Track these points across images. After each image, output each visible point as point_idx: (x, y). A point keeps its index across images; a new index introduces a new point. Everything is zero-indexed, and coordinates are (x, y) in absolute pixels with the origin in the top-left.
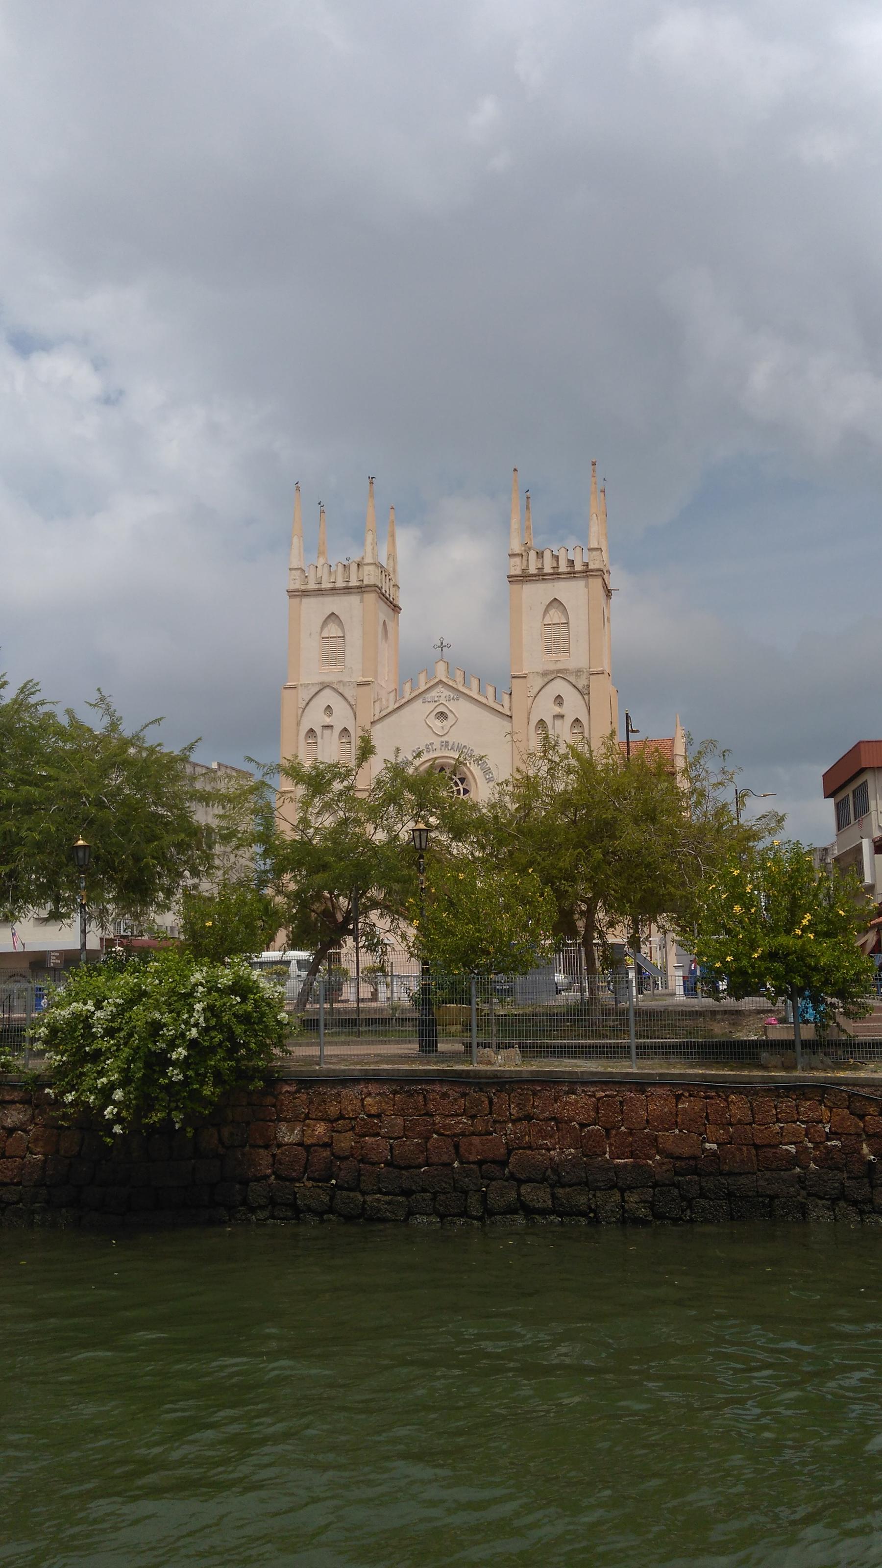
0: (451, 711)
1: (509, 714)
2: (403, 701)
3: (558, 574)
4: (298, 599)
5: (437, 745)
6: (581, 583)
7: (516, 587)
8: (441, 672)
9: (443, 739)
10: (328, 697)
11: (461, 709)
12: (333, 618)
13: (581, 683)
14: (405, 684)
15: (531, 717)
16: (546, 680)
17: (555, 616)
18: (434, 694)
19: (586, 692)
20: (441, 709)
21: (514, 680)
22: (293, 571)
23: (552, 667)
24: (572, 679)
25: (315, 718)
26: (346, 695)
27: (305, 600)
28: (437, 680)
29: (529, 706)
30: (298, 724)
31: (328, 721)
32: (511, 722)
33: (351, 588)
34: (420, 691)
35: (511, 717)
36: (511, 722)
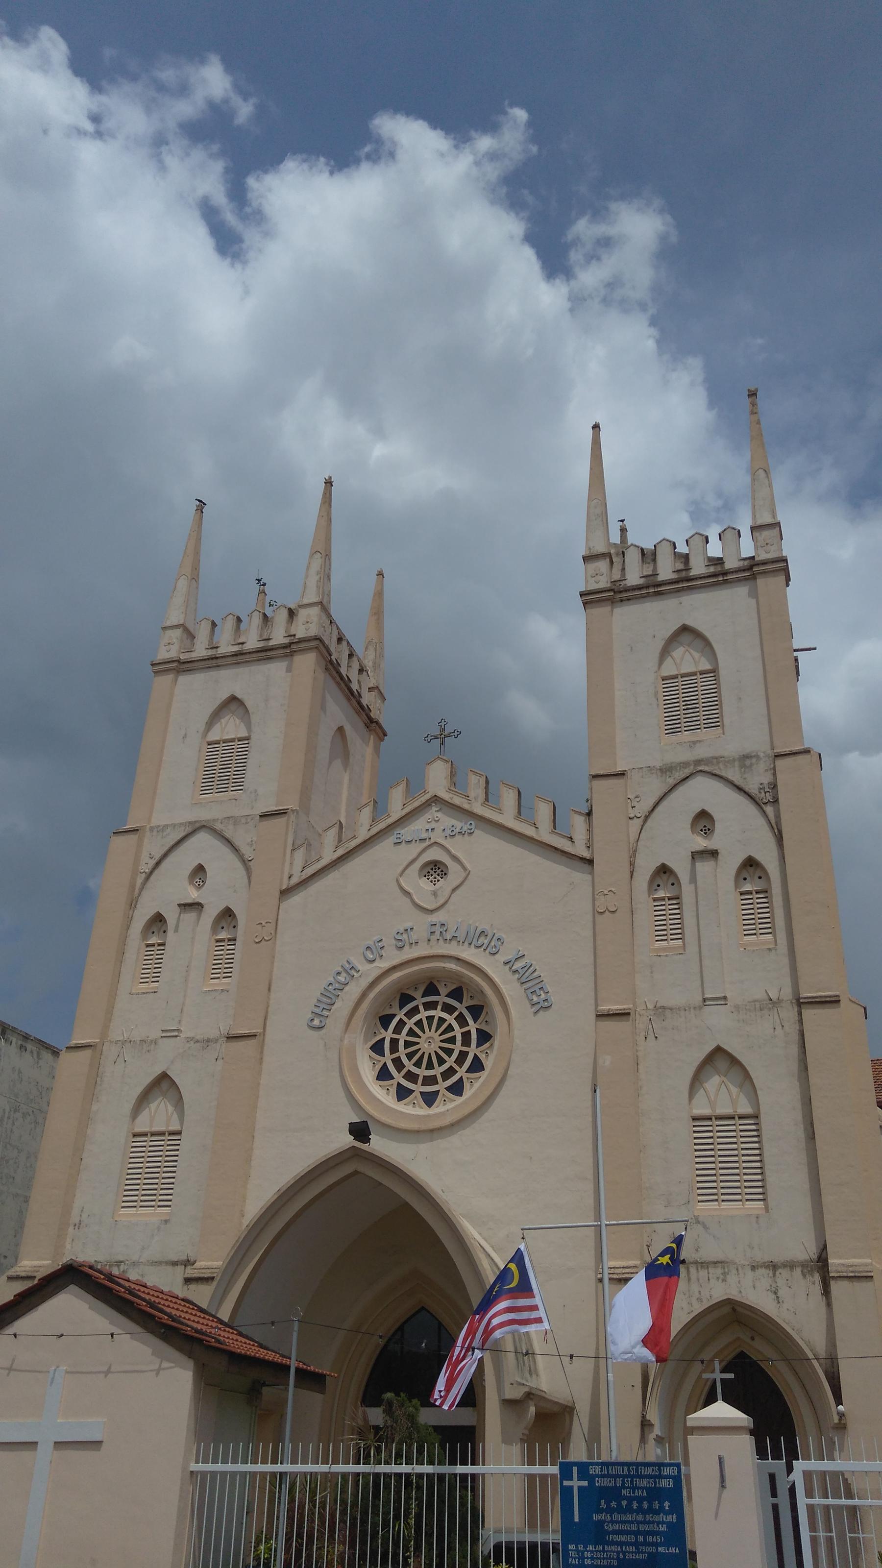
0: (455, 858)
1: (586, 854)
4: (170, 677)
6: (742, 591)
7: (603, 611)
8: (437, 779)
10: (202, 849)
12: (233, 706)
13: (756, 780)
14: (360, 809)
15: (640, 861)
16: (671, 781)
17: (686, 659)
18: (418, 826)
19: (769, 797)
21: (597, 783)
22: (169, 632)
23: (686, 755)
24: (733, 774)
25: (169, 889)
26: (238, 842)
27: (183, 679)
28: (427, 797)
29: (632, 839)
30: (133, 904)
31: (193, 895)
32: (592, 873)
33: (271, 649)
34: (390, 821)
35: (590, 862)
36: (592, 873)
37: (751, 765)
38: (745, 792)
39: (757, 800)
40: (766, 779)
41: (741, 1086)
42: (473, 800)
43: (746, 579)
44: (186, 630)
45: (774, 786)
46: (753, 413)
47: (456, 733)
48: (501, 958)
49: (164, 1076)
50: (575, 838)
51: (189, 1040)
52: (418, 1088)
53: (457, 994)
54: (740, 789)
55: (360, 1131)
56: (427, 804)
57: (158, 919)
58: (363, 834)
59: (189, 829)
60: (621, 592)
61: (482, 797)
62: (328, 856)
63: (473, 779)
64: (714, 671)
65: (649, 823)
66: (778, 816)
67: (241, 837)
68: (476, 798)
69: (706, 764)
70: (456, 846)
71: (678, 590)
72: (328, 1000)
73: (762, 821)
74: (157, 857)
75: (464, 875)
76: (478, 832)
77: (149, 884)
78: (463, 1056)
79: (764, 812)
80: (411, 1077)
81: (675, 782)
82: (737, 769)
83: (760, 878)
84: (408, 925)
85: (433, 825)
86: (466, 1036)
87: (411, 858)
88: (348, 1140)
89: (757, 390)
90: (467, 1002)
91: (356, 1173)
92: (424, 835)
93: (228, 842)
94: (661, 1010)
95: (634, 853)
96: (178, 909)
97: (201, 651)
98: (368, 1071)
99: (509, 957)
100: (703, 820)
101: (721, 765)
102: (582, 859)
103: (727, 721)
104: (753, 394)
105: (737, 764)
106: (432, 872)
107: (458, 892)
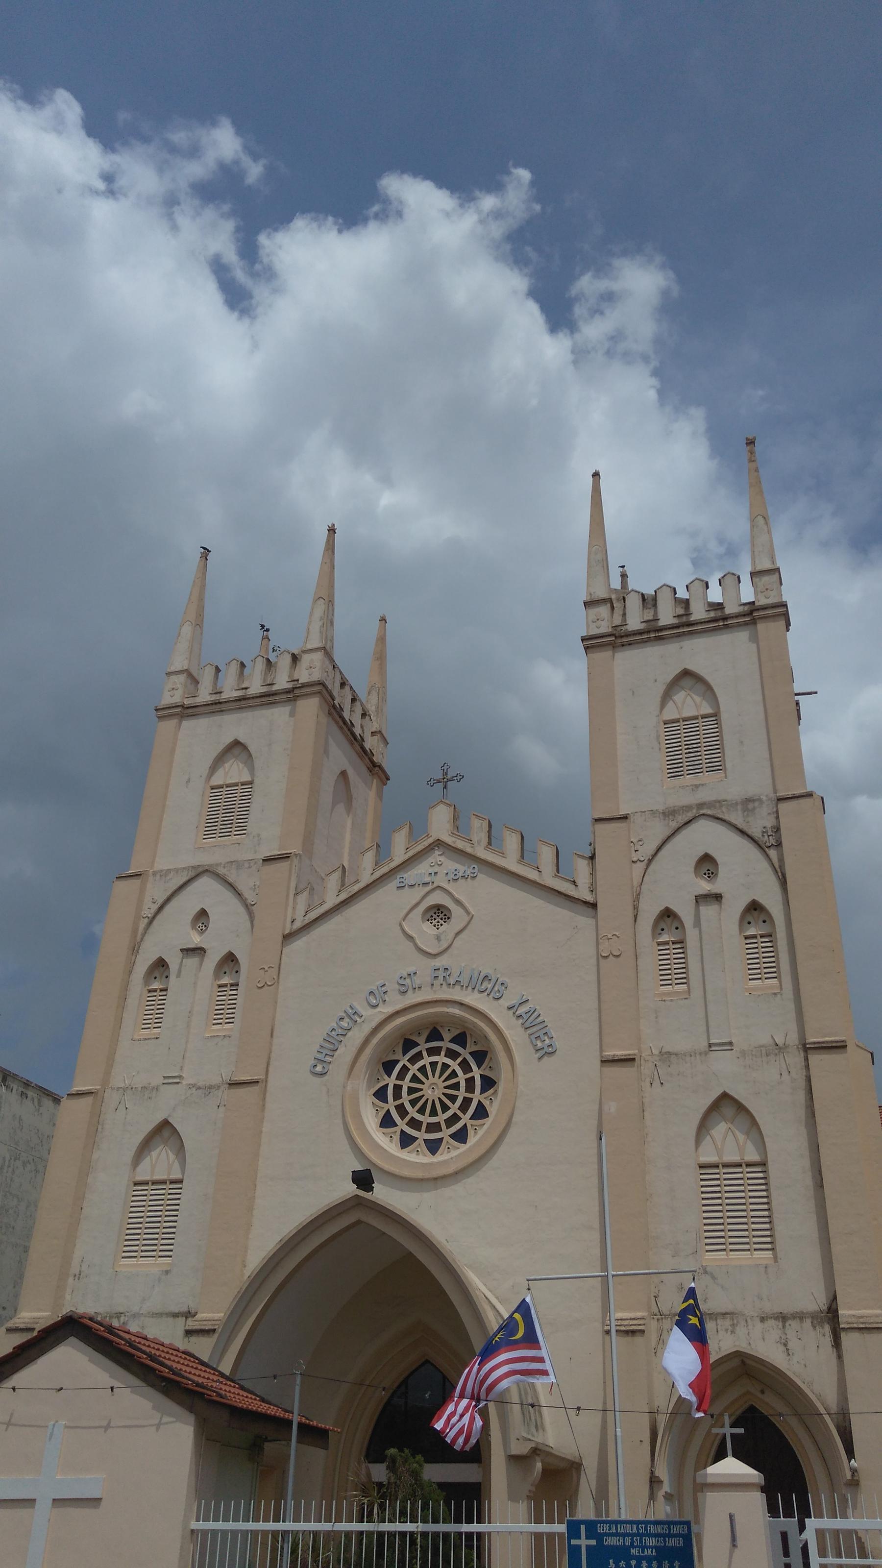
0: (458, 902)
1: (589, 898)
3: (689, 624)
4: (173, 722)
5: (424, 977)
6: (742, 636)
7: (603, 655)
8: (440, 823)
11: (482, 895)
12: (236, 751)
13: (759, 823)
14: (363, 853)
15: (642, 906)
16: (674, 825)
17: (688, 704)
18: (421, 871)
19: (772, 841)
20: (437, 898)
21: (600, 827)
22: (174, 678)
24: (737, 818)
25: (172, 934)
26: (241, 887)
27: (186, 724)
28: (430, 840)
29: (636, 881)
30: (135, 949)
31: (196, 940)
32: (595, 917)
34: (393, 865)
35: (594, 906)
36: (595, 917)
37: (754, 808)
38: (748, 836)
39: (760, 843)
40: (769, 822)
41: (747, 1134)
42: (476, 844)
43: (746, 624)
44: (190, 675)
45: (777, 829)
46: (751, 461)
47: (459, 777)
48: (505, 1003)
49: (166, 1124)
50: (579, 882)
51: (191, 1086)
52: (422, 1135)
53: (461, 1039)
54: (742, 832)
55: (363, 1179)
56: (430, 848)
57: (161, 964)
58: (366, 878)
59: (192, 874)
60: (622, 637)
61: (485, 841)
62: (331, 900)
63: (476, 823)
64: (716, 715)
65: (652, 867)
66: (781, 860)
67: (245, 882)
68: (479, 842)
69: (709, 808)
70: (459, 890)
71: (679, 635)
72: (332, 1043)
73: (765, 865)
74: (160, 901)
75: (467, 919)
76: (481, 876)
77: (152, 929)
78: (467, 1102)
79: (768, 855)
80: (414, 1124)
81: (677, 827)
82: (740, 812)
83: (764, 922)
84: (411, 970)
85: (436, 869)
86: (470, 1082)
87: (414, 902)
88: (351, 1189)
89: (755, 438)
90: (471, 1047)
91: (359, 1222)
92: (427, 879)
93: (231, 886)
94: (666, 1056)
95: (637, 897)
96: (180, 954)
97: (204, 696)
98: (371, 1119)
99: (514, 1001)
100: (707, 864)
101: (724, 809)
102: (586, 903)
103: (729, 765)
104: (751, 442)
105: (739, 807)
106: (435, 916)
107: (461, 936)
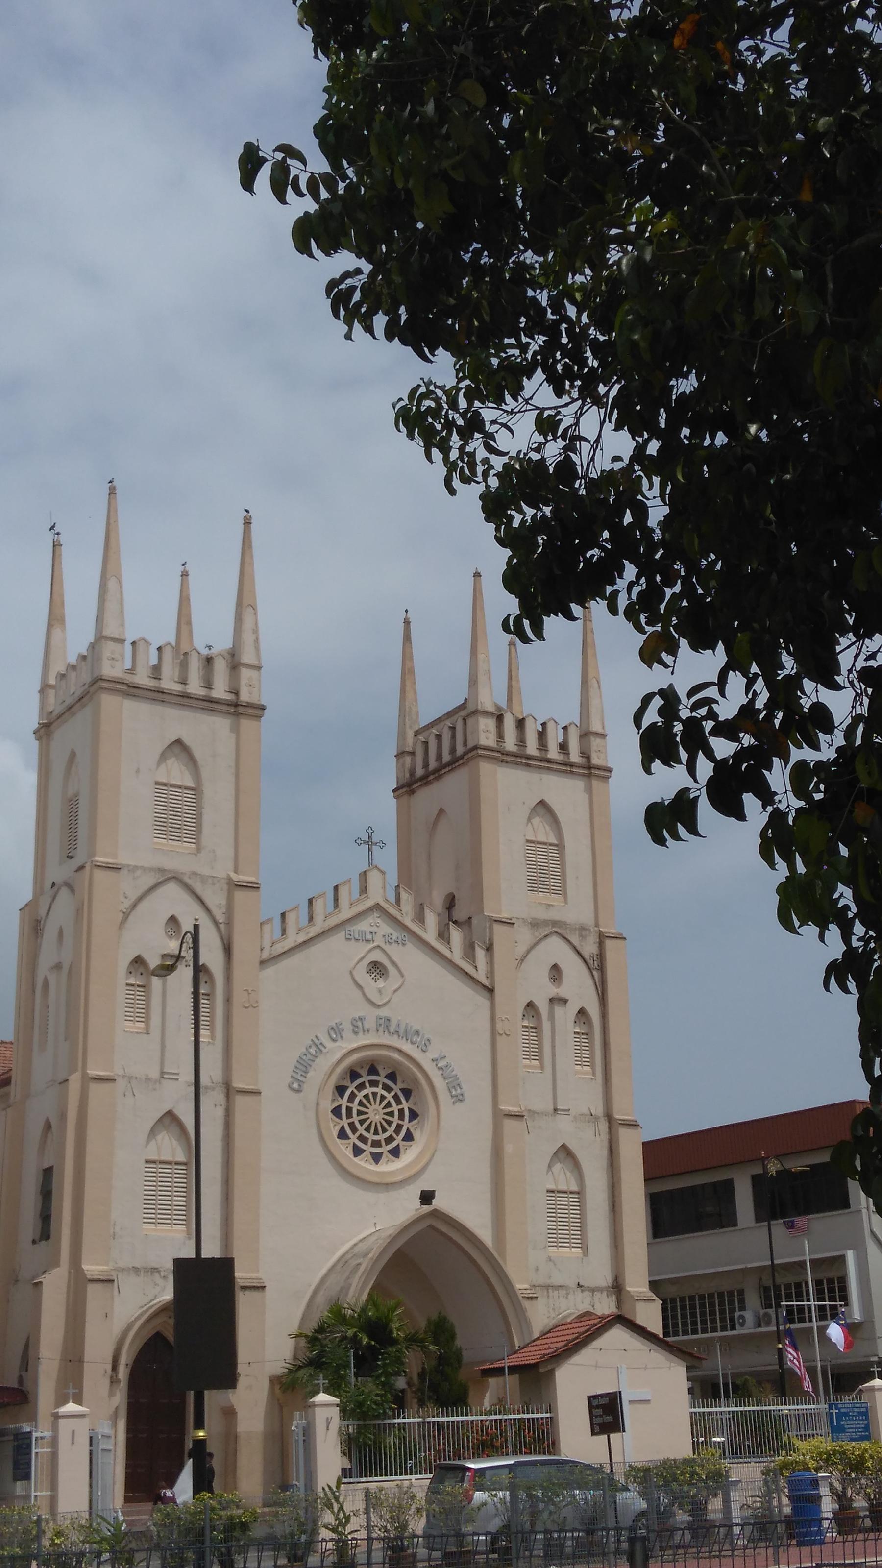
2: (313, 931)
5: (370, 1023)
9: (384, 1012)
11: (411, 959)
18: (364, 926)
41: (572, 1172)
53: (392, 1076)
70: (395, 951)
84: (361, 1014)
99: (436, 1056)
